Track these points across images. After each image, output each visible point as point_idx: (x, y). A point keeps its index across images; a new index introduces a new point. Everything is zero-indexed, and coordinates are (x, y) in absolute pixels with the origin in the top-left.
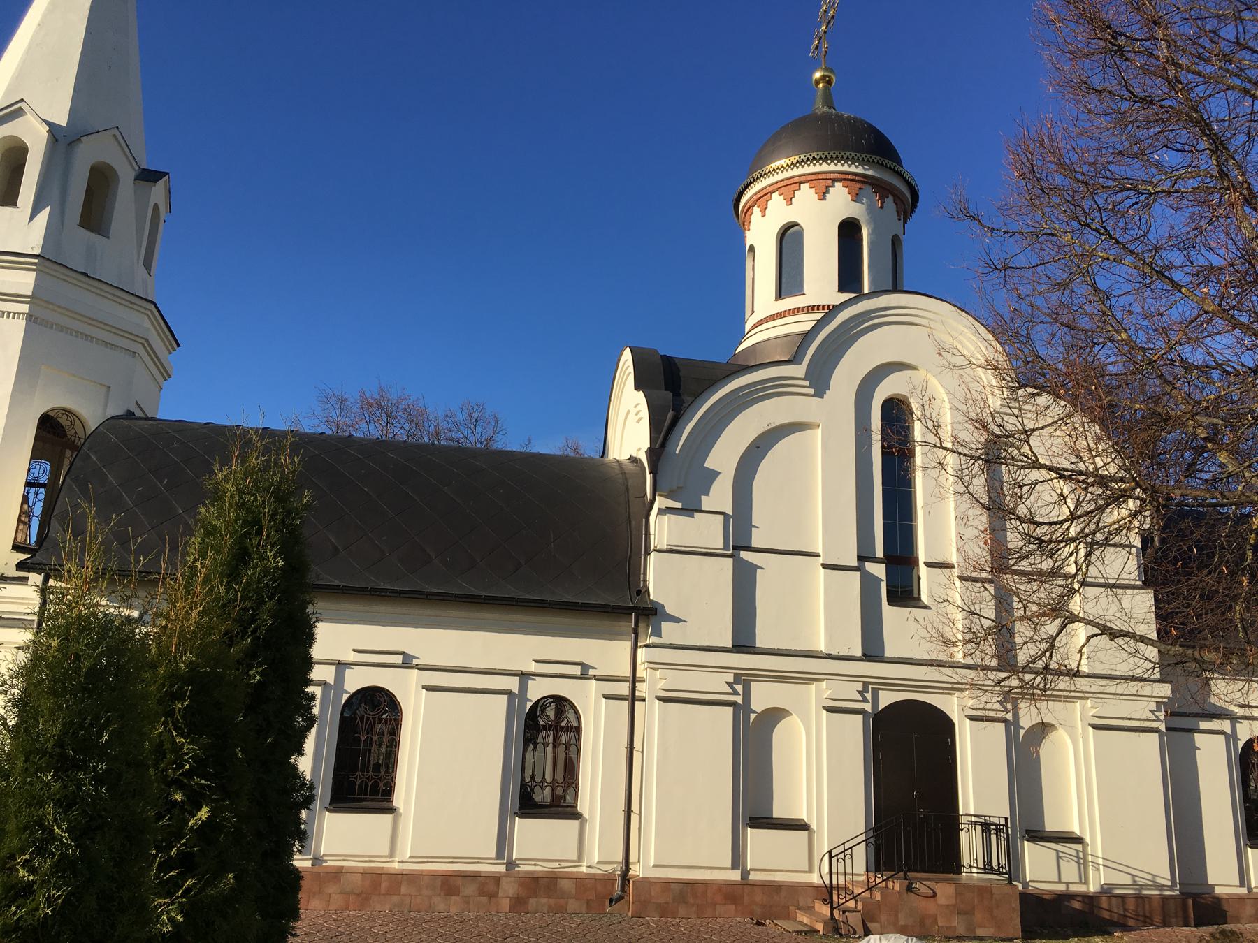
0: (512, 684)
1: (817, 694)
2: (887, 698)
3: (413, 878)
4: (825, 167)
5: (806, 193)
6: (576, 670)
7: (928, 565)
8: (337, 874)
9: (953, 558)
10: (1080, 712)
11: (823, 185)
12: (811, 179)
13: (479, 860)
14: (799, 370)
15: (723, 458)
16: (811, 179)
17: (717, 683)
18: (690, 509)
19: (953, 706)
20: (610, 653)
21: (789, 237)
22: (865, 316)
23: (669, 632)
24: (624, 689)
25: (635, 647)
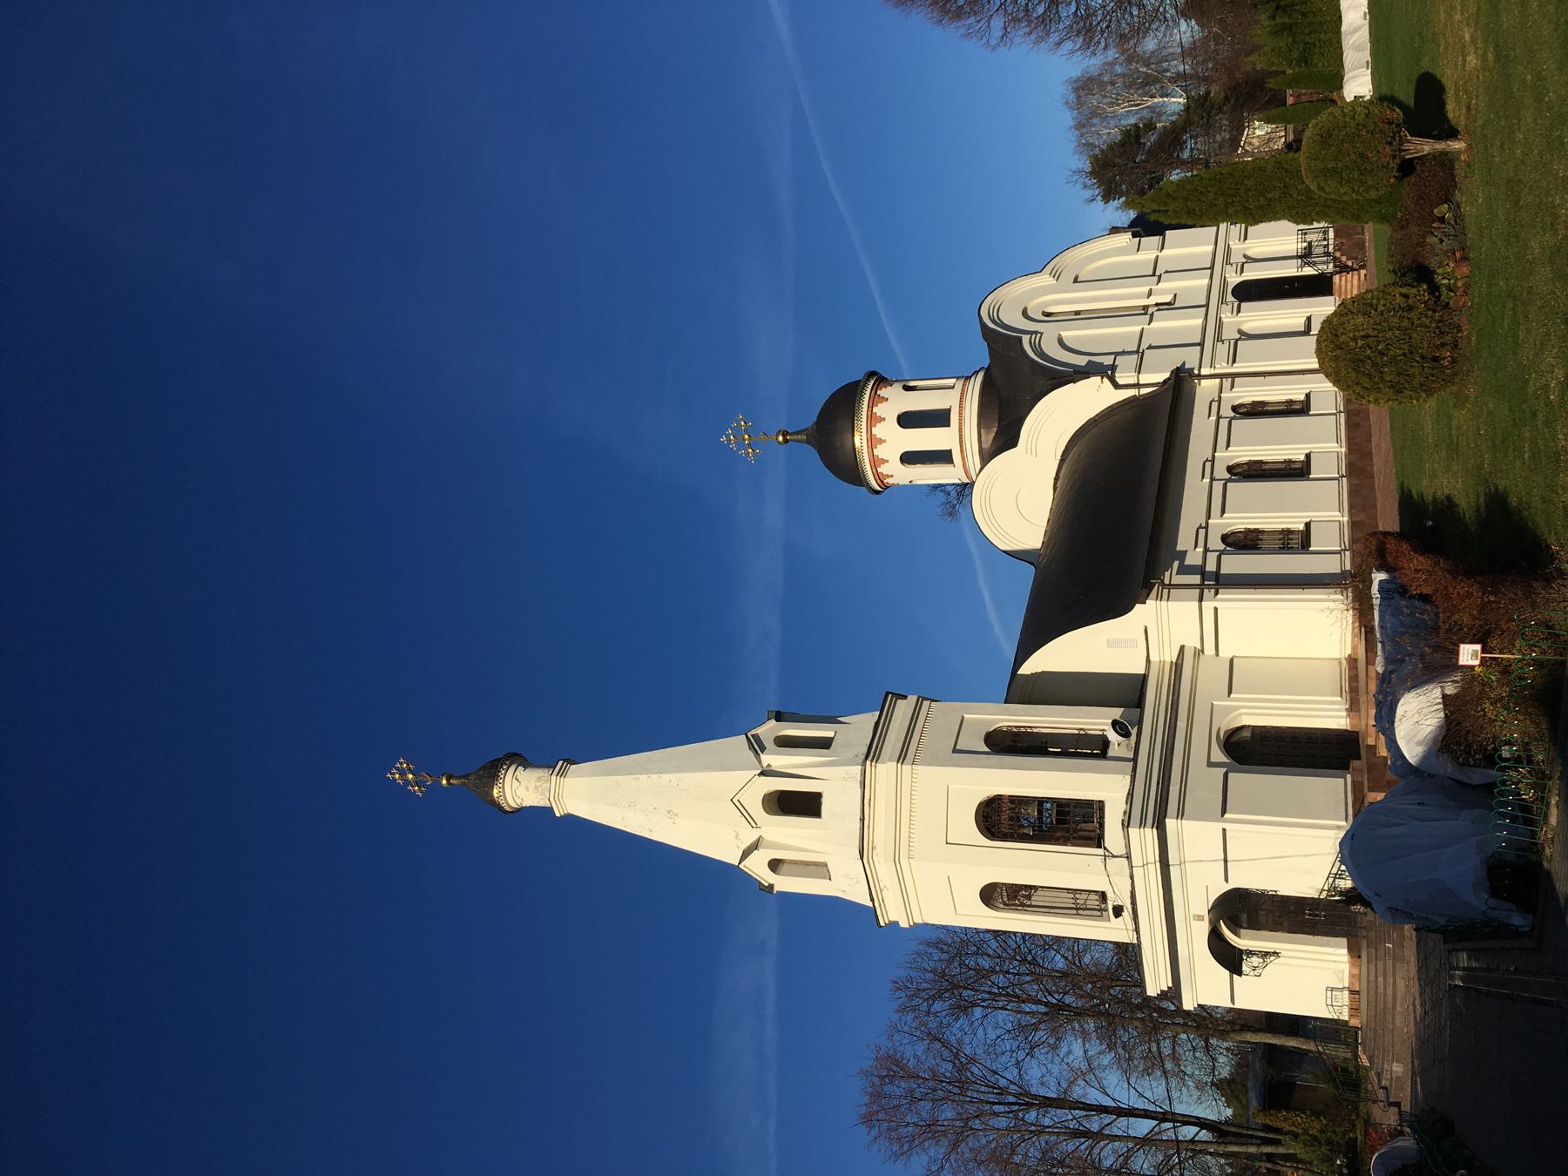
0: (1224, 424)
1: (1227, 318)
2: (1230, 298)
3: (1349, 439)
4: (866, 397)
5: (879, 410)
6: (1215, 405)
7: (1150, 294)
8: (1351, 467)
9: (1147, 289)
10: (1236, 246)
11: (875, 399)
12: (871, 405)
13: (1337, 423)
14: (1025, 339)
15: (1081, 361)
16: (871, 405)
17: (1222, 349)
18: (1113, 367)
19: (1234, 279)
20: (1206, 389)
21: (908, 420)
22: (993, 321)
23: (1192, 363)
24: (1227, 383)
25: (1200, 377)
